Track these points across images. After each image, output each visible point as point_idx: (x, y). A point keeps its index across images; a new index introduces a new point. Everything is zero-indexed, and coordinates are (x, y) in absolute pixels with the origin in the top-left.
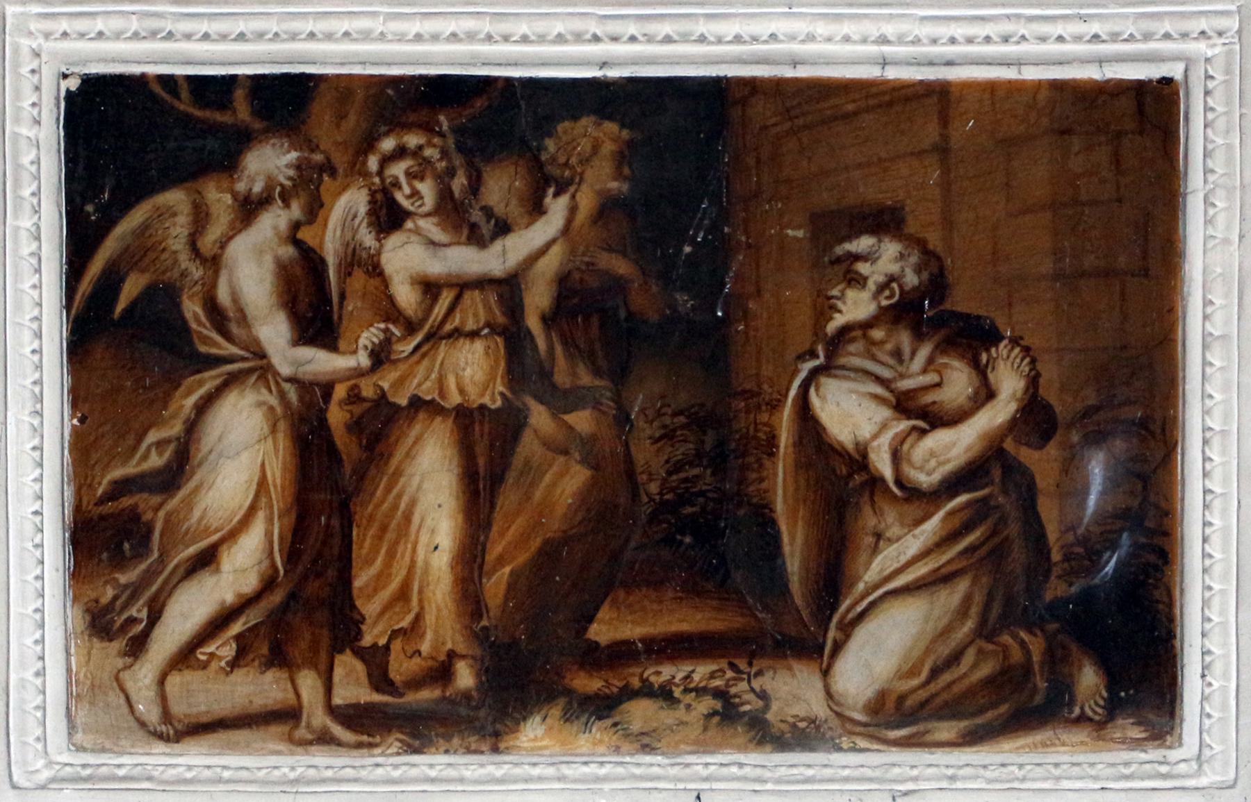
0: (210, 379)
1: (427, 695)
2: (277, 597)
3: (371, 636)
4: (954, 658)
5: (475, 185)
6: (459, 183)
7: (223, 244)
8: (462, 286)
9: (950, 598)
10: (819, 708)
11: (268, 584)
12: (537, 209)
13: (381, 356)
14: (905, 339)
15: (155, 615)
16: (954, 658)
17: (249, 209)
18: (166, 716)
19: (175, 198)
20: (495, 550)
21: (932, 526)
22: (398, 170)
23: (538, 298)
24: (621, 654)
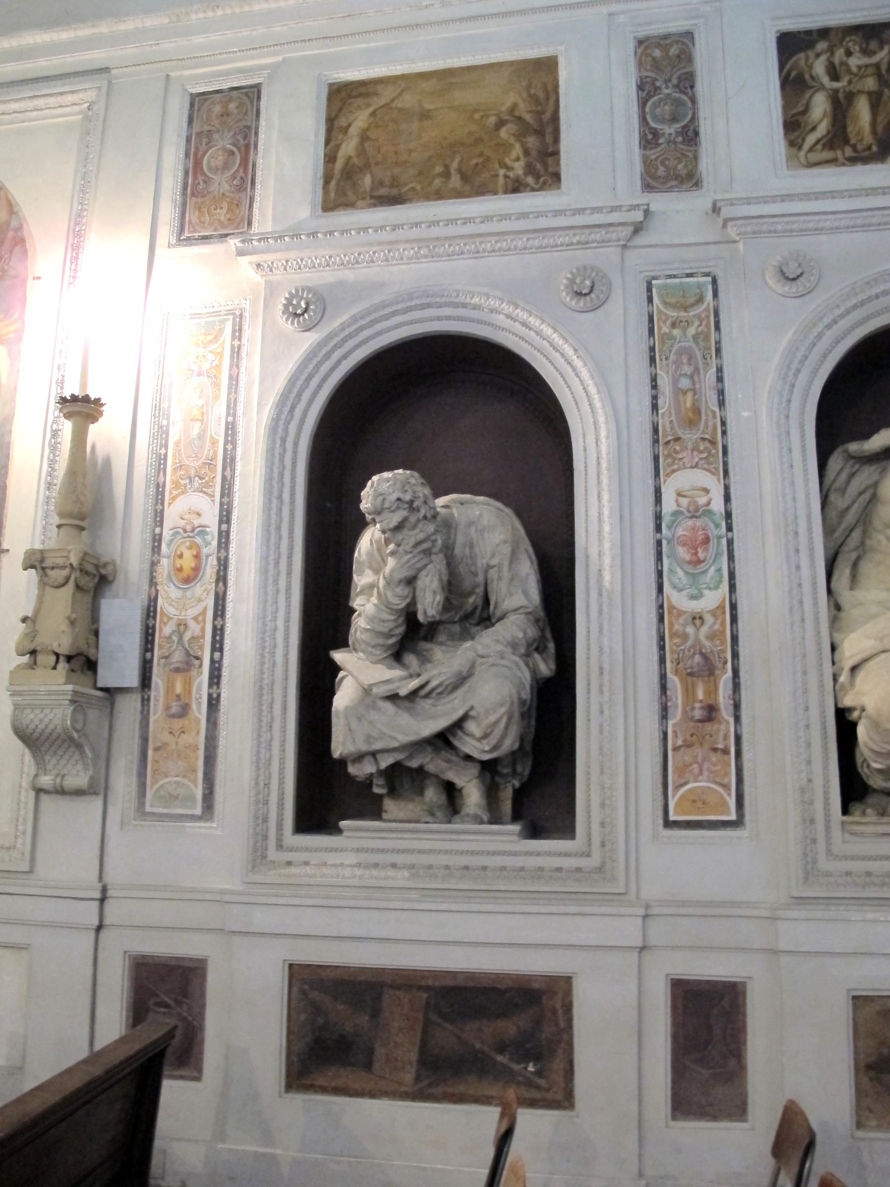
0: (812, 91)
1: (867, 153)
2: (830, 136)
3: (853, 141)
7: (812, 63)
11: (828, 133)
13: (850, 82)
15: (804, 140)
18: (808, 163)
20: (879, 119)
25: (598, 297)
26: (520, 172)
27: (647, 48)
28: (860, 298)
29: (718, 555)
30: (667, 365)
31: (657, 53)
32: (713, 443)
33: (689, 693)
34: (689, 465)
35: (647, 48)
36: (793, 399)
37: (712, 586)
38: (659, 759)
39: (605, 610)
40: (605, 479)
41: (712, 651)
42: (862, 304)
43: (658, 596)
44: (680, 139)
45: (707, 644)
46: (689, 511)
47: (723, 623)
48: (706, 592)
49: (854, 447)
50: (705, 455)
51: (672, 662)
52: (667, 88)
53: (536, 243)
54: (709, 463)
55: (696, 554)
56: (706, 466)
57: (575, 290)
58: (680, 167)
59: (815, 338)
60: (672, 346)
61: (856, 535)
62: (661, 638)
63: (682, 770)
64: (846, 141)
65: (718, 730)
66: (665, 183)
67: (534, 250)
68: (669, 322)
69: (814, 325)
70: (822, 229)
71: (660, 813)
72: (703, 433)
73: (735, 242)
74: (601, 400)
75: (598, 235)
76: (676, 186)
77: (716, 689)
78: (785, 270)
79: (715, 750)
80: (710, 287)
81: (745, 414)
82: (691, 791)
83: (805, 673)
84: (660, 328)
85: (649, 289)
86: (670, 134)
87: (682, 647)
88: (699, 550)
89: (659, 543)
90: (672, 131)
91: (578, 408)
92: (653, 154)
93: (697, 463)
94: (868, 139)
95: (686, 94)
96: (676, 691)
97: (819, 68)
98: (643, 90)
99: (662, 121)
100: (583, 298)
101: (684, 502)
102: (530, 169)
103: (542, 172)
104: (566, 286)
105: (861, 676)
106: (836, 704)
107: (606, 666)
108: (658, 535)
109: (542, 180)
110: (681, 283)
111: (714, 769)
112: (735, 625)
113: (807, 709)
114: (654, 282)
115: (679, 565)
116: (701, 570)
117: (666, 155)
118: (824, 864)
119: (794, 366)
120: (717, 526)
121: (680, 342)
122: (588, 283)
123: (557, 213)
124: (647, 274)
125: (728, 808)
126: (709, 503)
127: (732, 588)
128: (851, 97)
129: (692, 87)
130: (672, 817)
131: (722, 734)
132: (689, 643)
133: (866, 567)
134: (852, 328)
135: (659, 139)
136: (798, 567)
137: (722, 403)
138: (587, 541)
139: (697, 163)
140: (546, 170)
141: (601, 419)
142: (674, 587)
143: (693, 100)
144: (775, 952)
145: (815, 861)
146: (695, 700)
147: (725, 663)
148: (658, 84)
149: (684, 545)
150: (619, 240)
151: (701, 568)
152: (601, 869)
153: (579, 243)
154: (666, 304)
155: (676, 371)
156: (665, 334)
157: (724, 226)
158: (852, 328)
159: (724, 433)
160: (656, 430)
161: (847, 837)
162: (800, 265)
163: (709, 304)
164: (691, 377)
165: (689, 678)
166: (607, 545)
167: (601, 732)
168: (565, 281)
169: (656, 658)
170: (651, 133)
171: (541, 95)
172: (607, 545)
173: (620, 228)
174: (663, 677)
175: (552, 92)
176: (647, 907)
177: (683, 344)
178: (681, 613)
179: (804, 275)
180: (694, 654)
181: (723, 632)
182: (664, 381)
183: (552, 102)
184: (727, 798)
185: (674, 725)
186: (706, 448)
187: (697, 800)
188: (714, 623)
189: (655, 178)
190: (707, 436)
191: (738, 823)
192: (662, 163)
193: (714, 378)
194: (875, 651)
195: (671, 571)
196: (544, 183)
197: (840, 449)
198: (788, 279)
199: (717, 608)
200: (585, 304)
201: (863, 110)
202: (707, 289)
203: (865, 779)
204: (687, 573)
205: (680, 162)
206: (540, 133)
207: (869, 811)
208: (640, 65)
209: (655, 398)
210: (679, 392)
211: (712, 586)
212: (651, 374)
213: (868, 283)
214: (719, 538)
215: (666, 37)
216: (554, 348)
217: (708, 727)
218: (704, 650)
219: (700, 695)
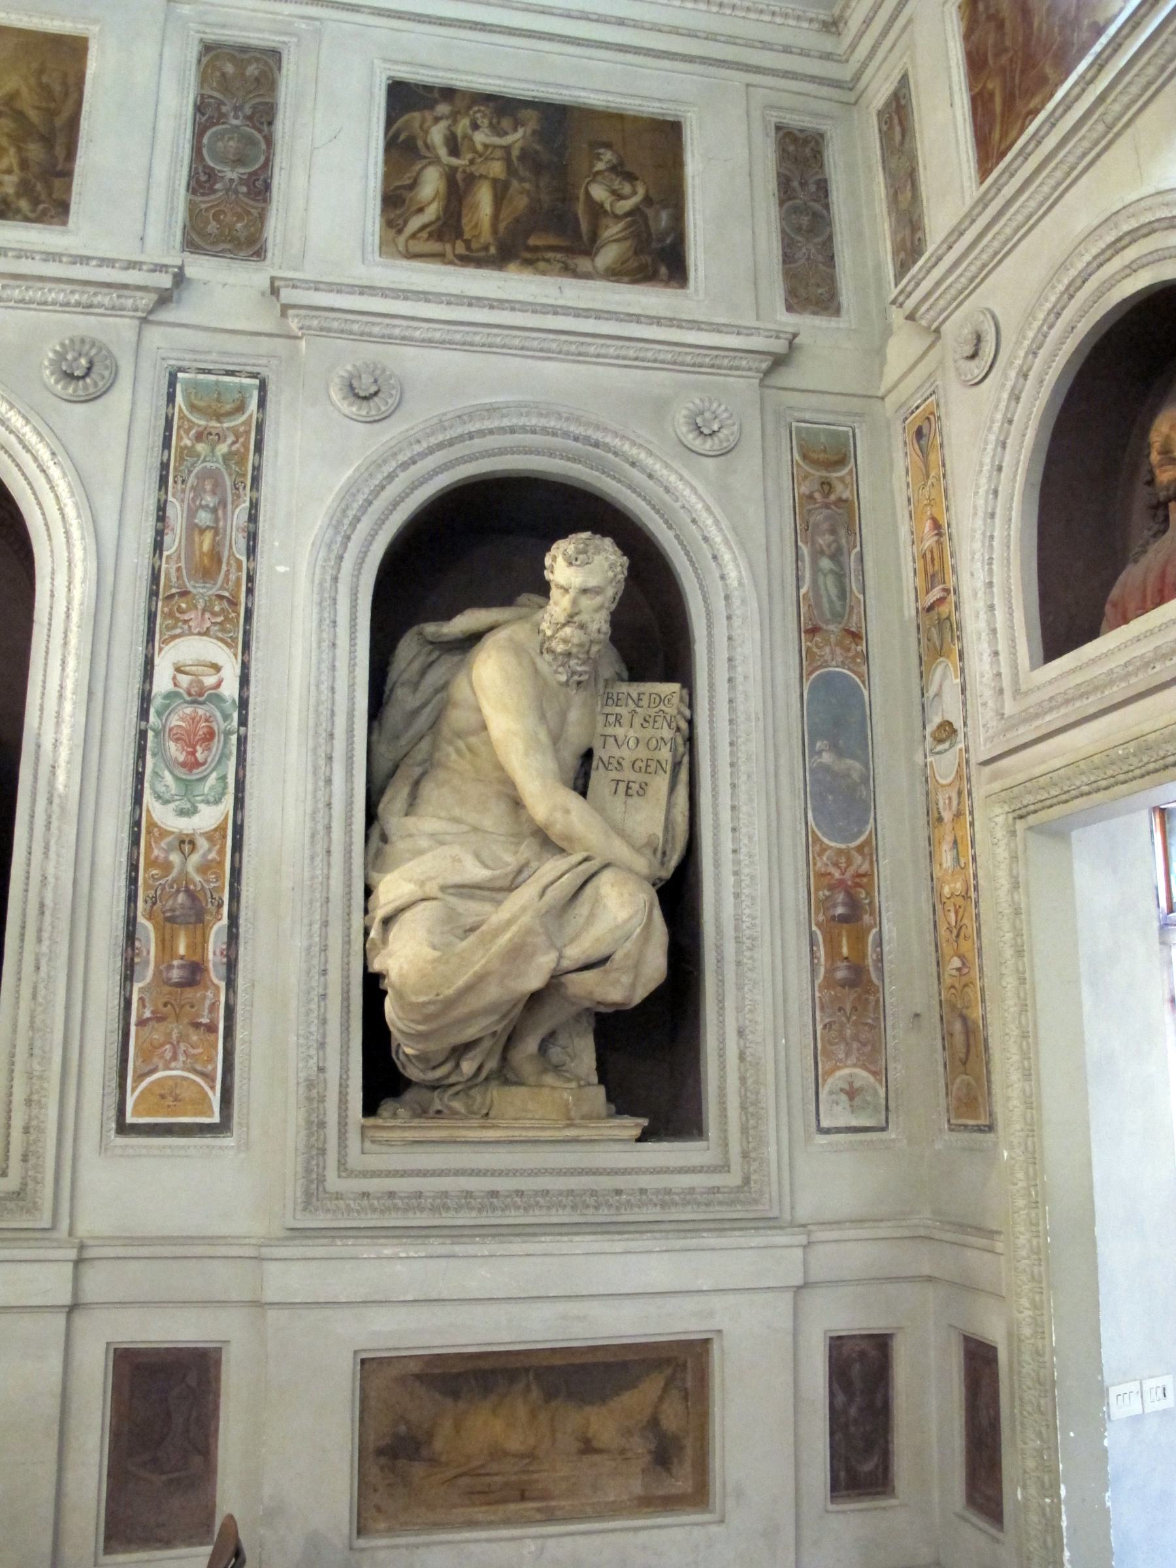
0: (424, 162)
1: (482, 254)
2: (440, 223)
3: (467, 236)
4: (628, 260)
5: (499, 123)
6: (495, 121)
7: (429, 128)
8: (495, 147)
9: (628, 243)
10: (590, 269)
11: (438, 219)
12: (515, 130)
13: (472, 162)
14: (614, 177)
15: (406, 223)
16: (628, 260)
17: (437, 120)
19: (417, 115)
20: (501, 217)
21: (621, 225)
22: (478, 115)
23: (515, 153)
24: (536, 249)
25: (96, 384)
26: (10, 190)
27: (217, 57)
28: (449, 435)
29: (224, 757)
30: (183, 491)
31: (229, 68)
32: (233, 603)
33: (166, 945)
34: (196, 631)
35: (217, 57)
36: (346, 555)
37: (212, 799)
38: (116, 1038)
39: (55, 824)
40: (73, 640)
41: (203, 888)
42: (451, 442)
43: (134, 809)
44: (244, 189)
45: (198, 878)
46: (189, 694)
47: (221, 852)
48: (201, 807)
49: (430, 629)
50: (220, 619)
51: (146, 902)
52: (236, 117)
53: (16, 293)
54: (223, 630)
55: (193, 753)
56: (220, 635)
57: (64, 368)
58: (239, 225)
59: (385, 478)
60: (193, 465)
61: (425, 745)
62: (133, 867)
63: (147, 1053)
64: (459, 233)
65: (204, 998)
66: (214, 243)
67: (12, 304)
68: (193, 432)
69: (385, 461)
70: (411, 339)
71: (112, 1113)
72: (222, 588)
73: (296, 338)
74: (81, 527)
75: (105, 298)
76: (230, 251)
77: (205, 941)
78: (355, 383)
79: (197, 1025)
80: (255, 394)
81: (281, 569)
82: (158, 1082)
84: (179, 438)
85: (172, 384)
86: (232, 180)
87: (162, 882)
88: (198, 748)
89: (143, 735)
90: (234, 176)
91: (49, 535)
92: (205, 202)
93: (208, 629)
94: (486, 235)
95: (260, 131)
96: (148, 940)
97: (437, 135)
98: (203, 114)
99: (223, 161)
100: (74, 382)
101: (184, 680)
102: (25, 188)
103: (43, 197)
104: (52, 362)
105: (395, 931)
106: (365, 967)
107: (49, 902)
108: (143, 724)
109: (41, 207)
110: (217, 383)
111: (193, 1051)
112: (237, 855)
114: (180, 375)
115: (167, 767)
116: (198, 777)
117: (222, 207)
118: (333, 1181)
119: (351, 513)
120: (226, 717)
121: (204, 461)
122: (83, 362)
123: (51, 256)
124: (172, 362)
125: (210, 1107)
126: (218, 685)
127: (239, 803)
128: (472, 179)
129: (270, 123)
130: (130, 1119)
131: (208, 1003)
132: (174, 873)
133: (429, 790)
134: (436, 472)
135: (215, 183)
137: (251, 551)
138: (40, 723)
139: (262, 225)
140: (50, 195)
141: (78, 553)
142: (158, 797)
143: (269, 141)
144: (258, 1305)
145: (321, 1180)
146: (173, 954)
147: (220, 906)
148: (224, 109)
149: (177, 740)
150: (136, 310)
151: (197, 773)
152: (18, 1195)
153: (78, 304)
154: (193, 407)
155: (194, 500)
156: (186, 447)
157: (284, 314)
158: (436, 472)
159: (250, 591)
160: (155, 577)
161: (368, 1145)
162: (376, 381)
163: (251, 416)
164: (214, 511)
165: (168, 925)
166: (66, 730)
167: (34, 996)
168: (51, 355)
169: (123, 894)
170: (205, 173)
171: (57, 88)
172: (66, 730)
173: (139, 294)
174: (131, 922)
175: (74, 86)
176: (82, 1247)
177: (208, 465)
178: (164, 833)
179: (380, 395)
180: (178, 891)
181: (221, 863)
182: (176, 513)
183: (71, 102)
184: (210, 1093)
185: (141, 990)
186: (223, 610)
187: (167, 1095)
188: (210, 850)
189: (202, 234)
190: (226, 594)
191: (222, 1127)
192: (216, 217)
193: (245, 517)
194: (413, 899)
195: (156, 774)
196: (44, 213)
197: (415, 629)
198: (357, 396)
199: (216, 830)
200: (75, 391)
201: (484, 198)
202: (251, 396)
203: (401, 1069)
204: (177, 779)
205: (240, 218)
206: (47, 141)
207: (401, 1111)
208: (203, 79)
209: (160, 534)
210: (192, 528)
211: (212, 799)
212: (159, 501)
213: (459, 417)
214: (228, 734)
215: (244, 49)
216: (25, 447)
217: (189, 993)
218: (192, 887)
219: (182, 950)
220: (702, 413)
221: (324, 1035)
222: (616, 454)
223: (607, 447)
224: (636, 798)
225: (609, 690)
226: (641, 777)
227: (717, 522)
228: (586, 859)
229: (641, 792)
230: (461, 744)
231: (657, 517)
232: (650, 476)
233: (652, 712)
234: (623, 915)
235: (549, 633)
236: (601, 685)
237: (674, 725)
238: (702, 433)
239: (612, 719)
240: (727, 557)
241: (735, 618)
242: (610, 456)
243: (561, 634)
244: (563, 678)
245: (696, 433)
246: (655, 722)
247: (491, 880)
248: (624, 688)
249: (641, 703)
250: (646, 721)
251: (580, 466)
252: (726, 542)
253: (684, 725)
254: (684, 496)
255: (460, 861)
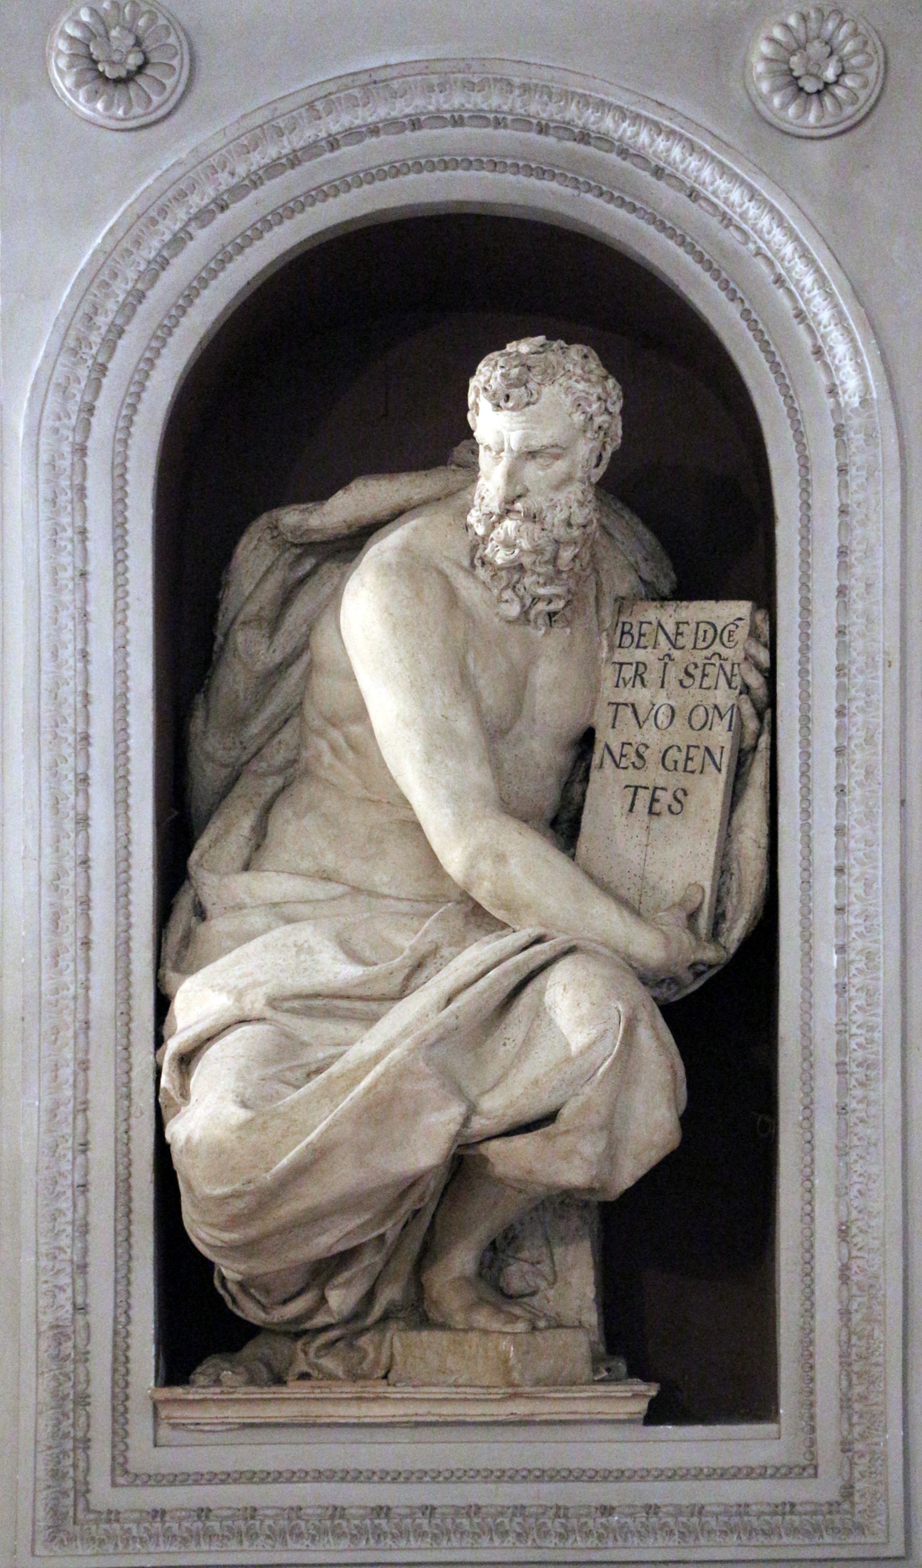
83: (84, 1066)
113: (85, 1147)
136: (83, 821)
220: (802, 47)
221: (85, 1251)
222: (624, 153)
223: (604, 140)
224: (667, 818)
225: (623, 619)
226: (675, 780)
227: (822, 281)
228: (539, 940)
229: (676, 807)
230: (336, 735)
231: (706, 277)
232: (693, 195)
233: (700, 657)
234: (578, 1039)
235: (480, 530)
236: (607, 613)
237: (737, 681)
238: (801, 89)
239: (628, 672)
240: (840, 348)
241: (853, 471)
242: (613, 158)
243: (499, 533)
244: (514, 610)
245: (790, 90)
246: (704, 675)
247: (363, 984)
248: (652, 613)
249: (681, 641)
250: (687, 673)
251: (554, 185)
252: (840, 318)
253: (755, 681)
254: (759, 233)
255: (310, 951)
